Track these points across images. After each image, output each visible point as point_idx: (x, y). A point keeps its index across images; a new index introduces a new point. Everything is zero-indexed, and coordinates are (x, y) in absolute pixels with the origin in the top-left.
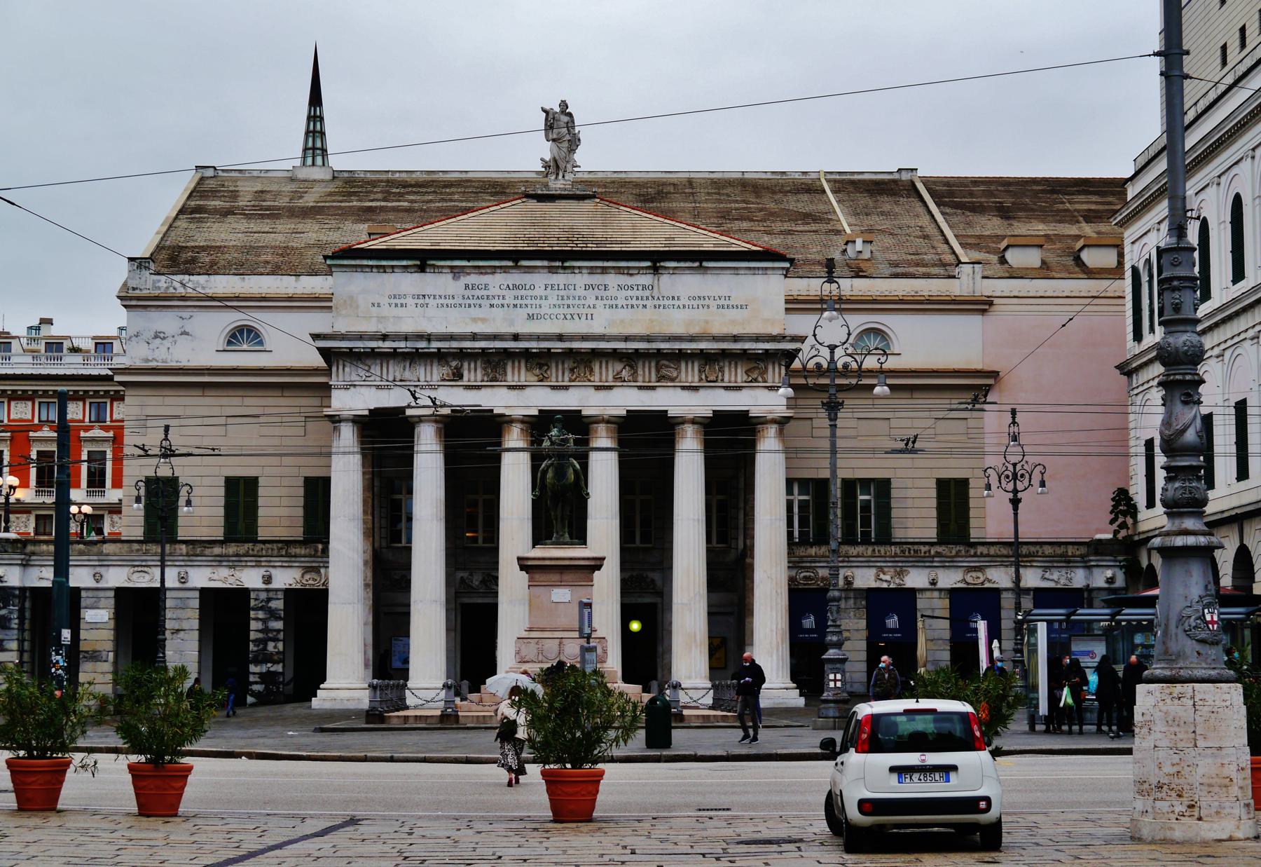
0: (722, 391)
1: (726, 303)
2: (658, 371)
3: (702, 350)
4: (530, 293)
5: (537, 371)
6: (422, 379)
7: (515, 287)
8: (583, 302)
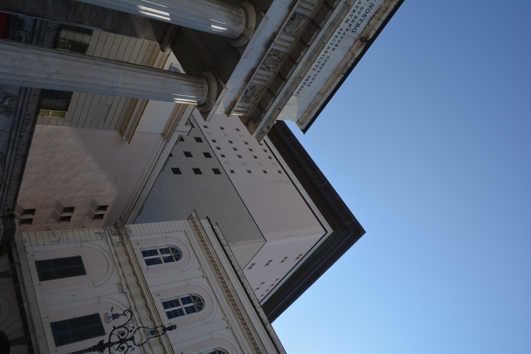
0: (252, 65)
1: (308, 83)
2: (300, 14)
3: (297, 64)
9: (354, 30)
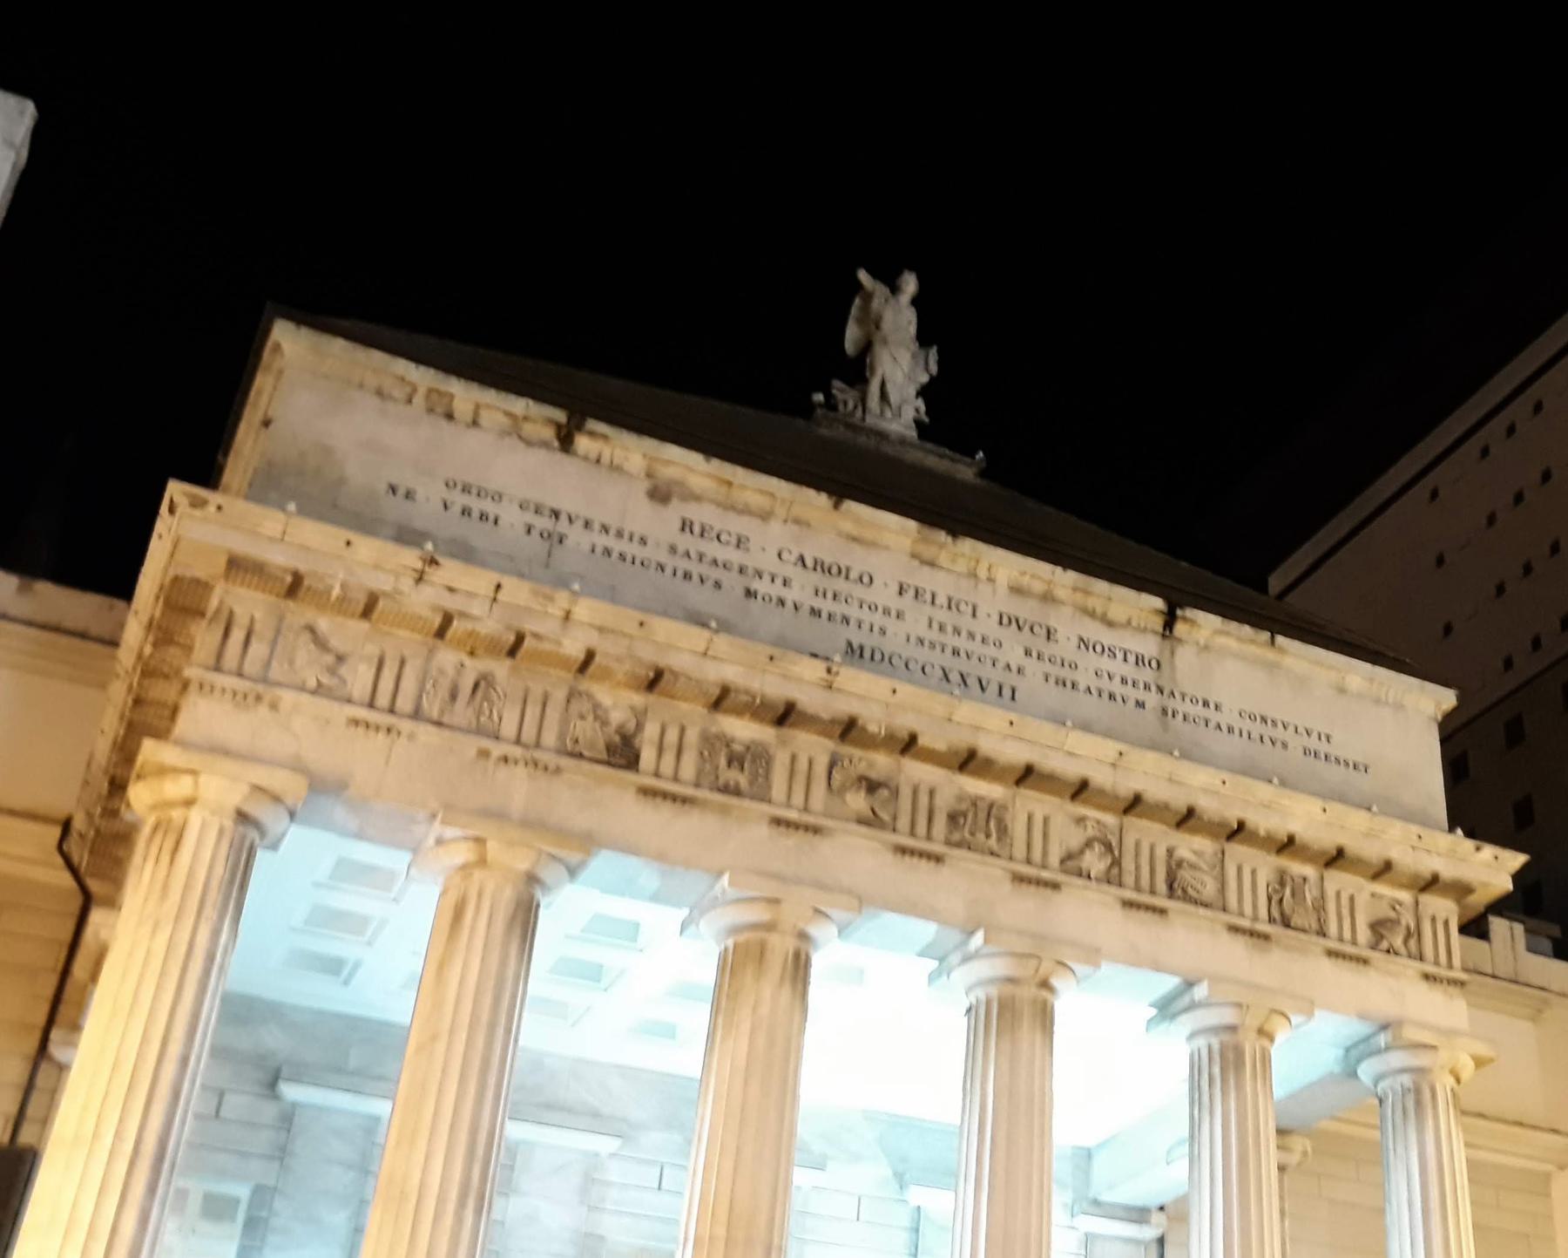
1: (1323, 748)
4: (859, 591)
5: (858, 801)
6: (509, 728)
7: (819, 565)
8: (991, 651)
9: (1154, 664)
